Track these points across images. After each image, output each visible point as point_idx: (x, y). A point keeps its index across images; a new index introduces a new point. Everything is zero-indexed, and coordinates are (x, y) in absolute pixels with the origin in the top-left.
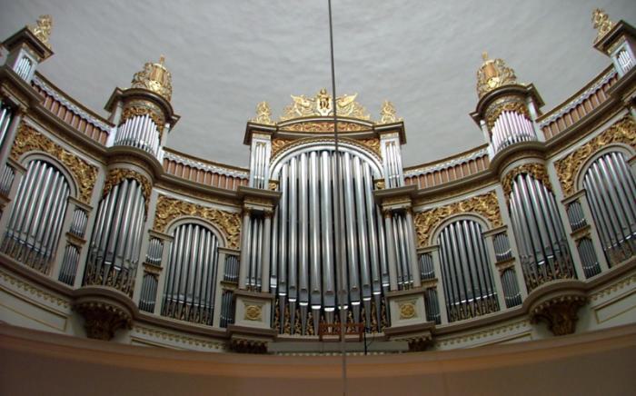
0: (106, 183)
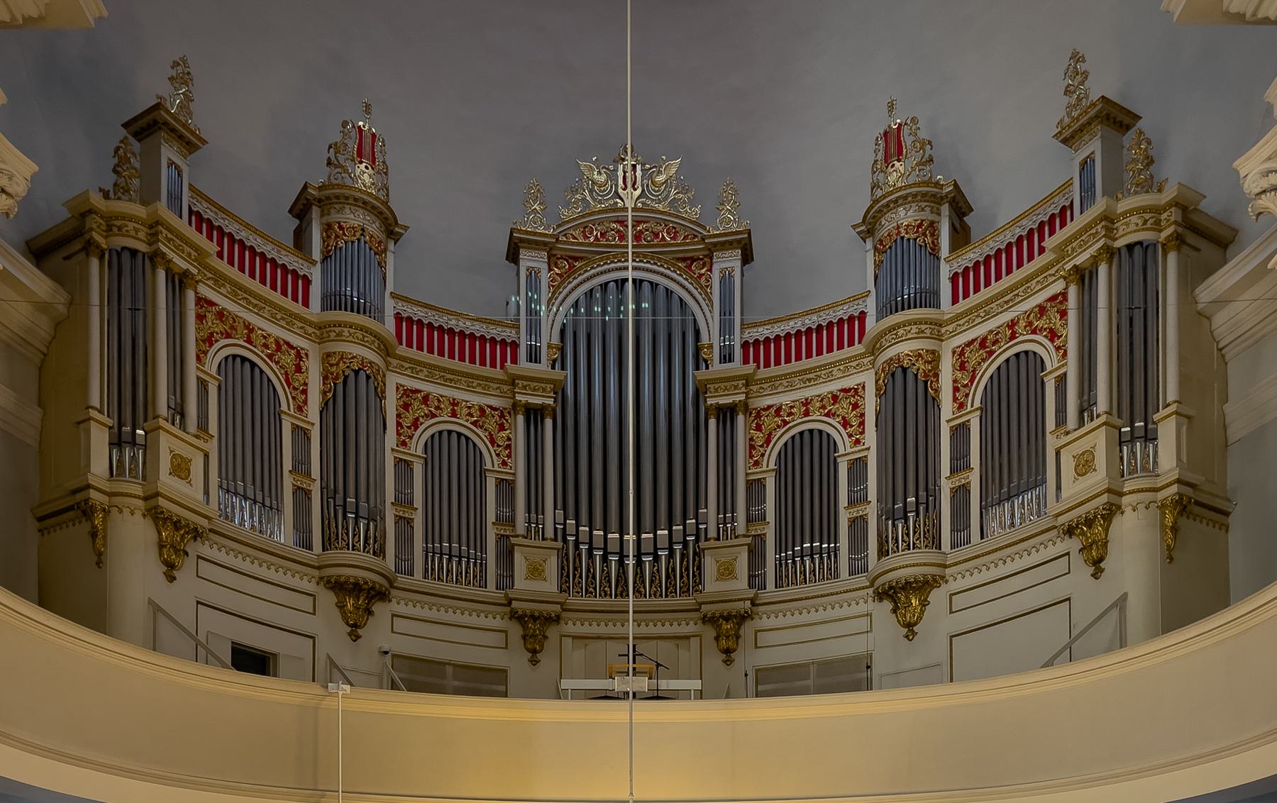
0: (325, 378)
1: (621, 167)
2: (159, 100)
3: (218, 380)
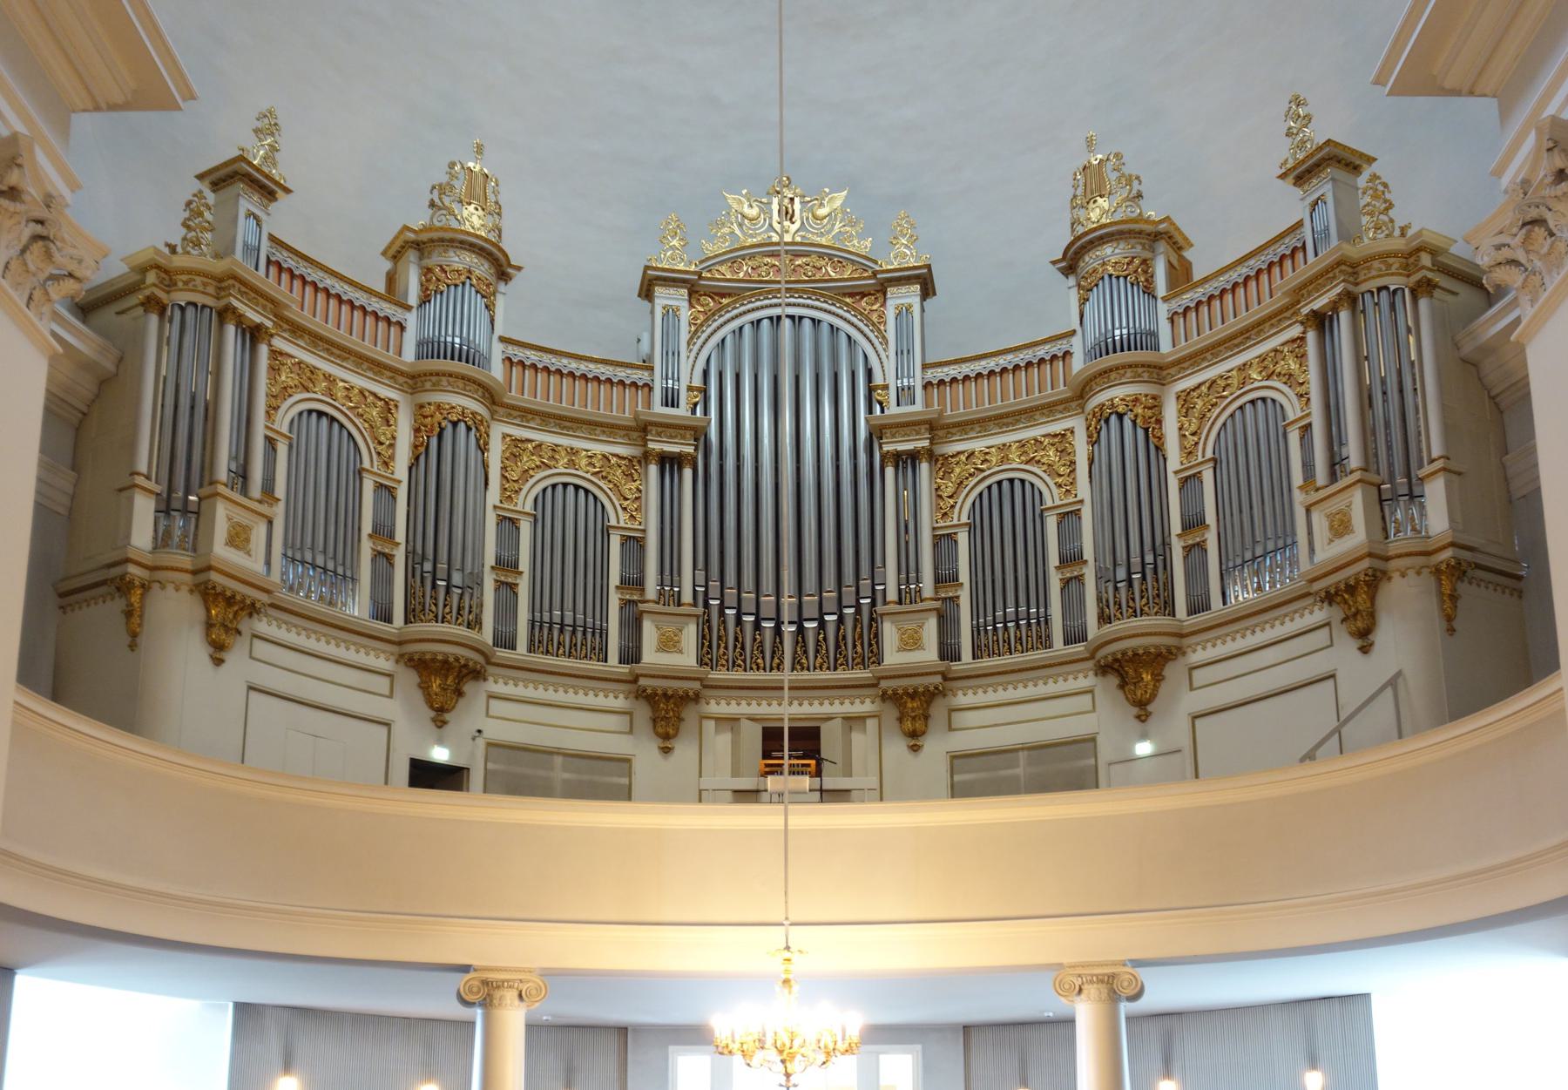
0: (417, 430)
1: (775, 201)
2: (241, 152)
3: (290, 438)
